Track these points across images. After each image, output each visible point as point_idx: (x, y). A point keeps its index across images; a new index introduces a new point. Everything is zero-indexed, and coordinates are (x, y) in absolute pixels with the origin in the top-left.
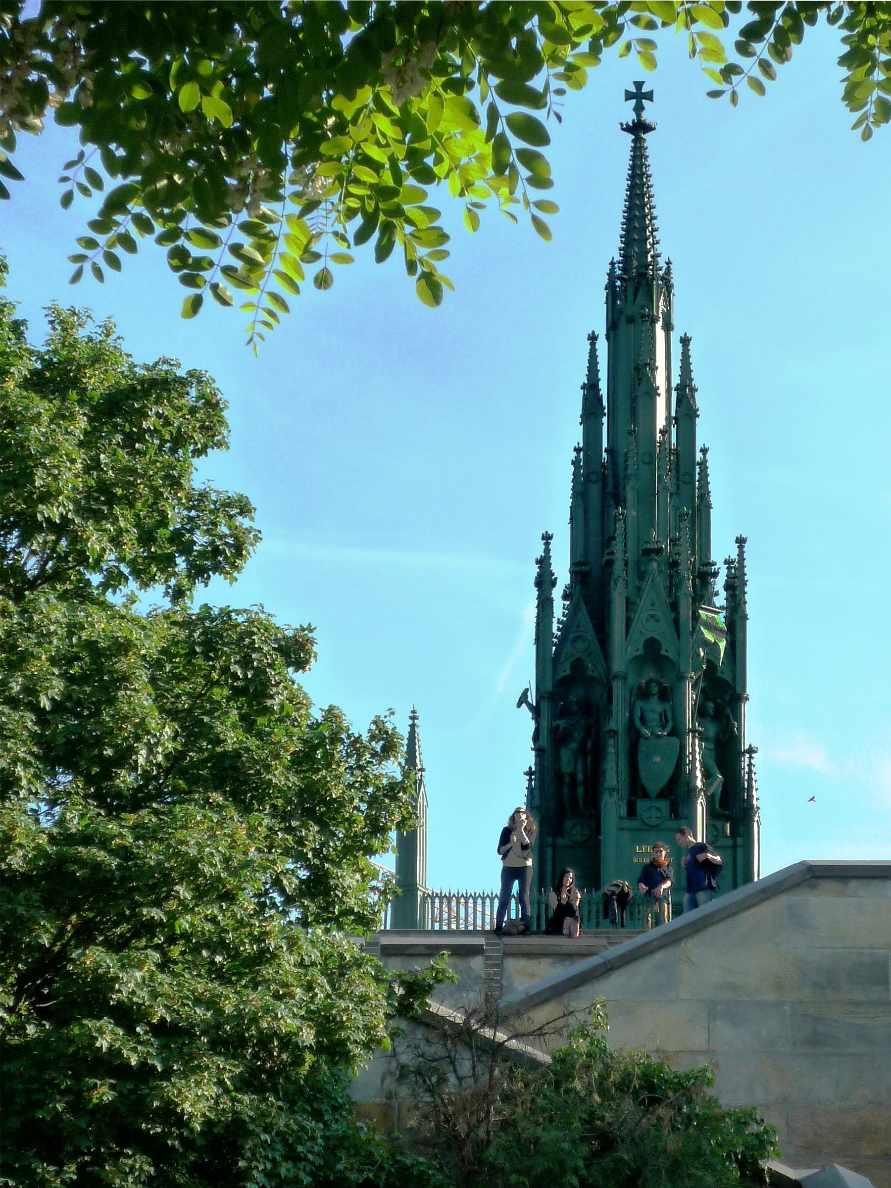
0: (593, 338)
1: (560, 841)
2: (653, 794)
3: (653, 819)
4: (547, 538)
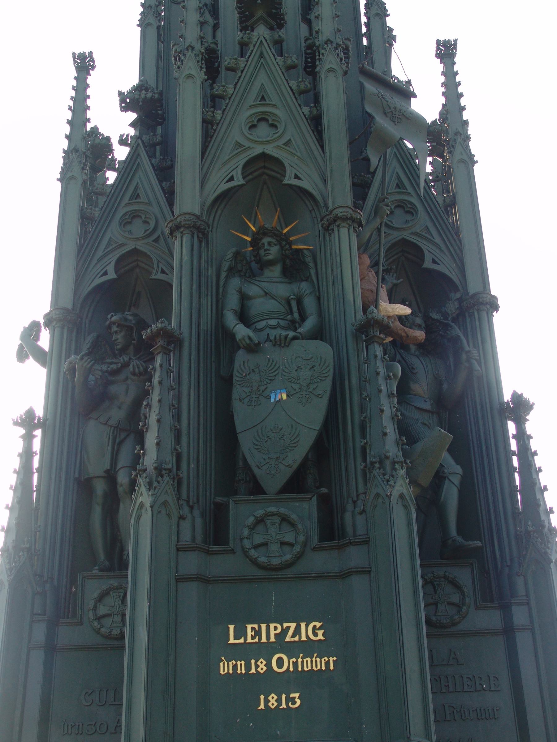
2: (273, 482)
3: (274, 547)
4: (84, 64)
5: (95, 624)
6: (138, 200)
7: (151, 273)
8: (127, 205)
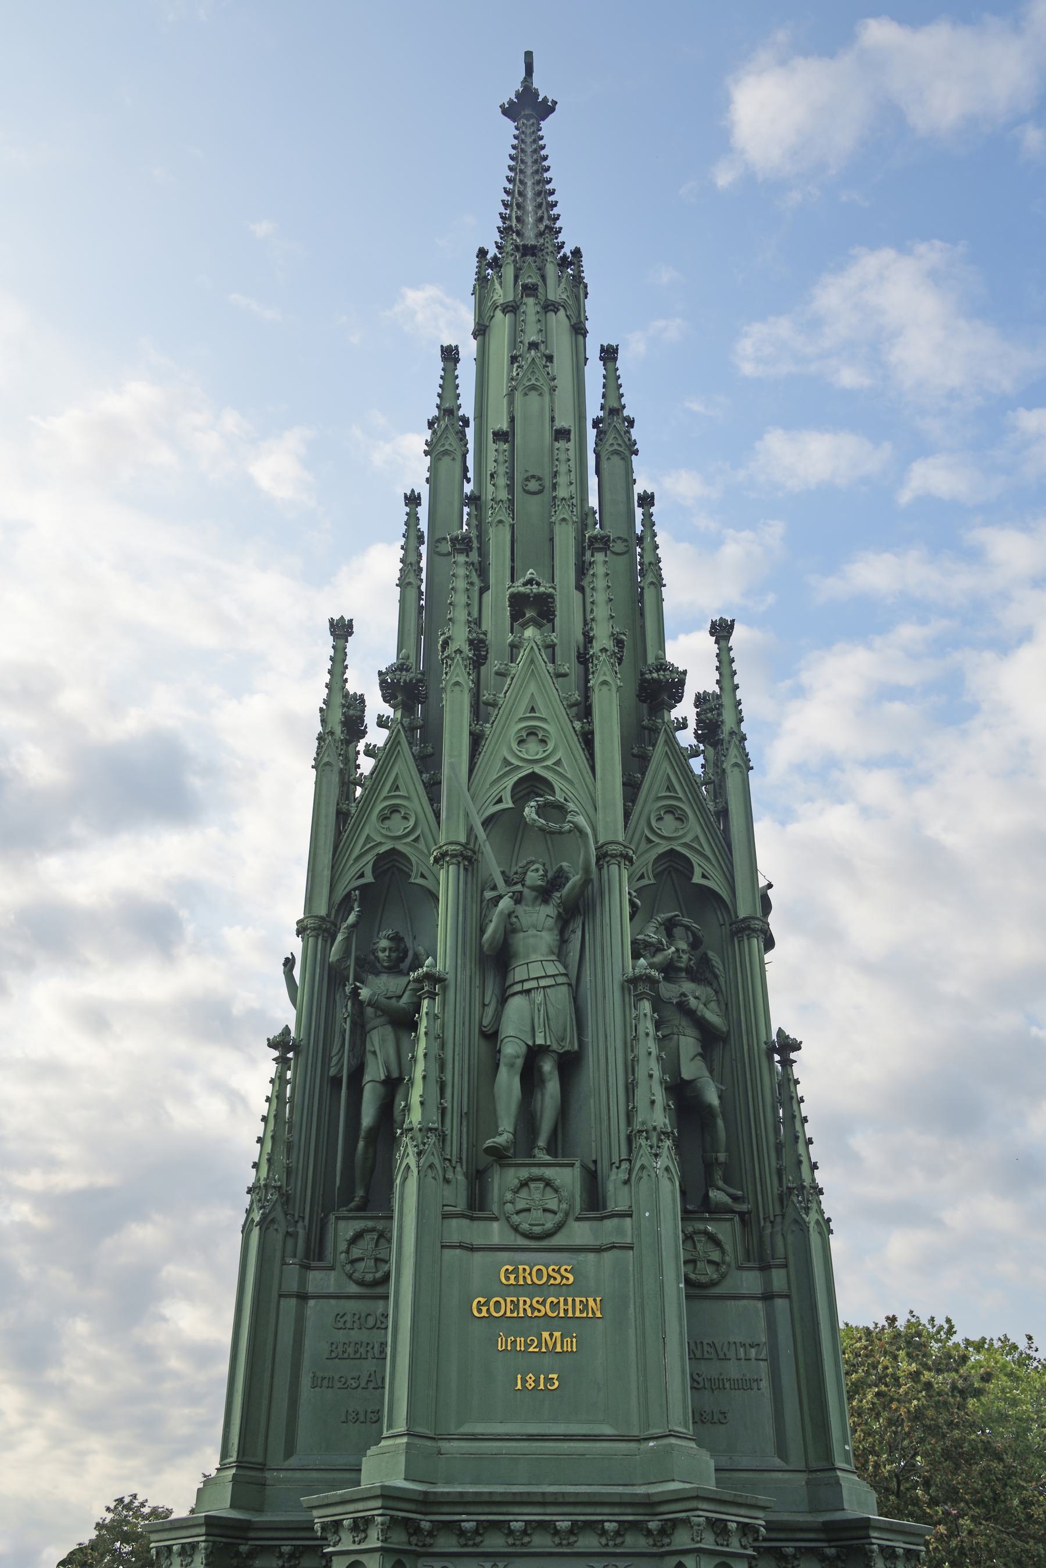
0: (450, 355)
1: (318, 1280)
3: (537, 1214)
5: (348, 1267)
6: (396, 793)
7: (410, 876)
8: (386, 798)
